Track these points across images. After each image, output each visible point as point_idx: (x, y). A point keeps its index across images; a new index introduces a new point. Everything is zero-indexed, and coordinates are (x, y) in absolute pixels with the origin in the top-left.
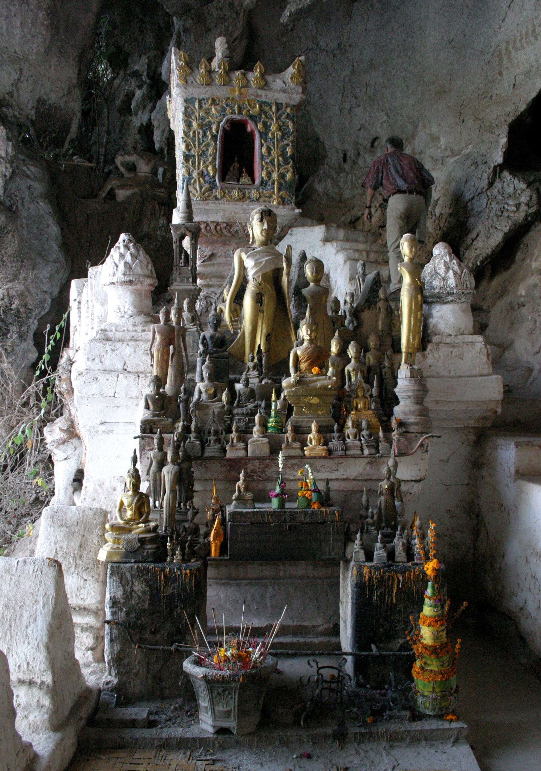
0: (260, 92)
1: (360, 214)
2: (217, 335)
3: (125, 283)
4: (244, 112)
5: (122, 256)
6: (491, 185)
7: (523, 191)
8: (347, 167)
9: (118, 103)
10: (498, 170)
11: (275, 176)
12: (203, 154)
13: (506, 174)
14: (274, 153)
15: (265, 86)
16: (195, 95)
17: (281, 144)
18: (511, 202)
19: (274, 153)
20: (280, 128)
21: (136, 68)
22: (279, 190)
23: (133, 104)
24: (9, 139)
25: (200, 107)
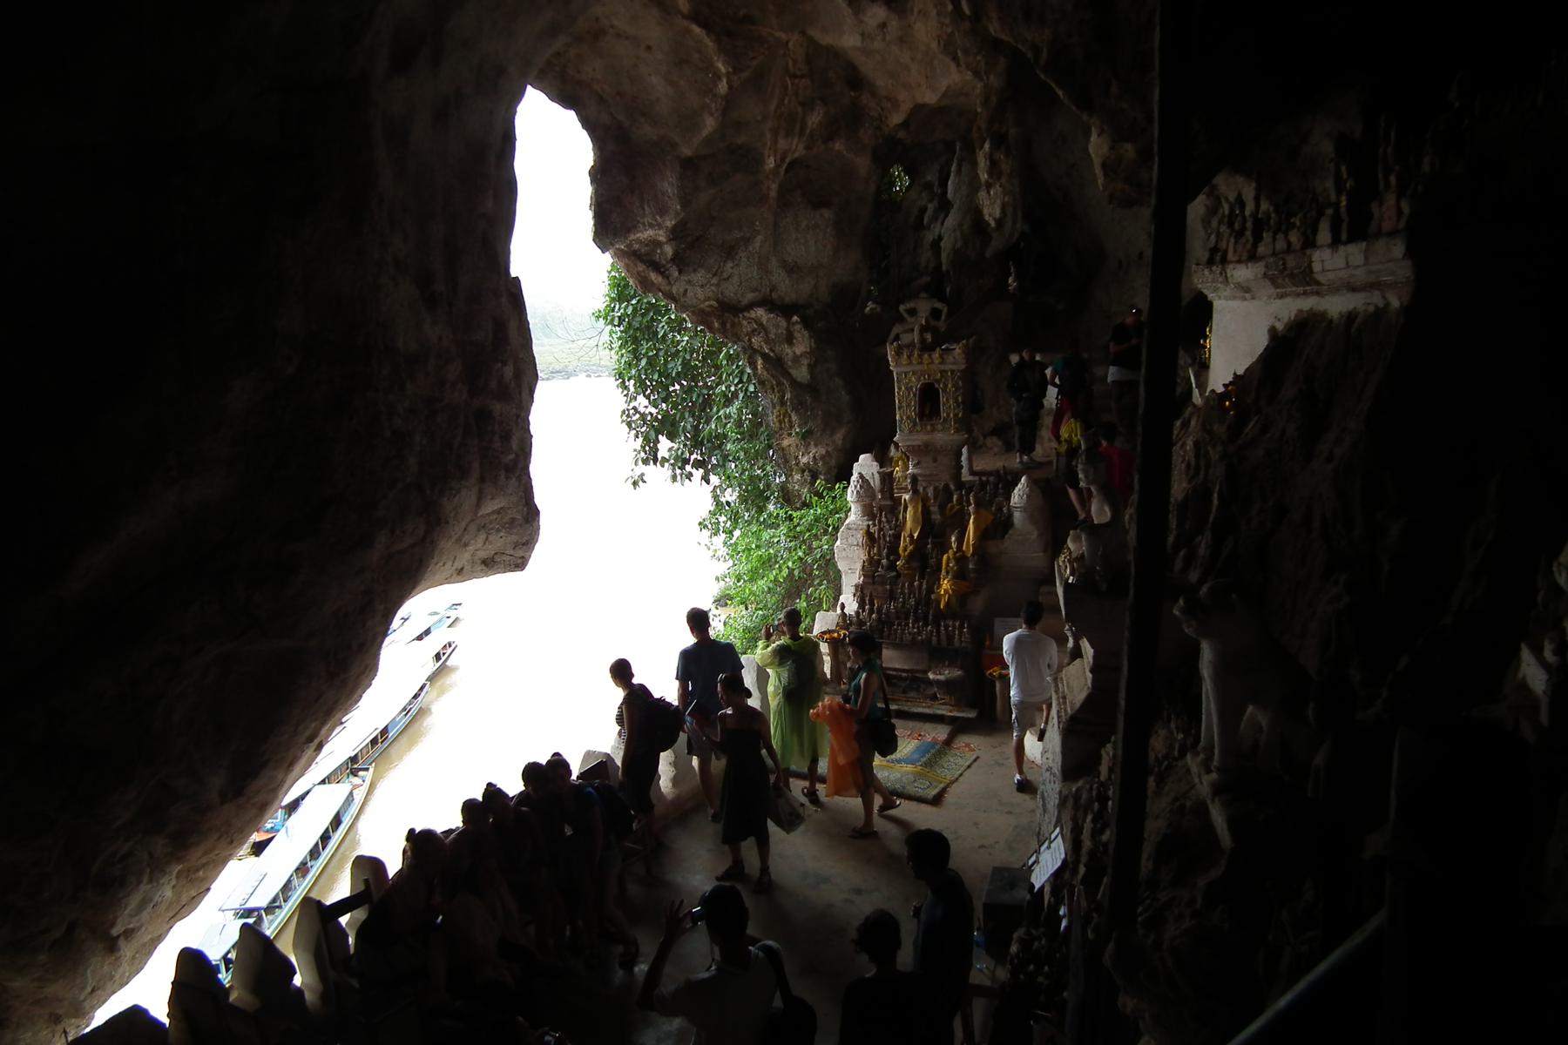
12: (909, 405)
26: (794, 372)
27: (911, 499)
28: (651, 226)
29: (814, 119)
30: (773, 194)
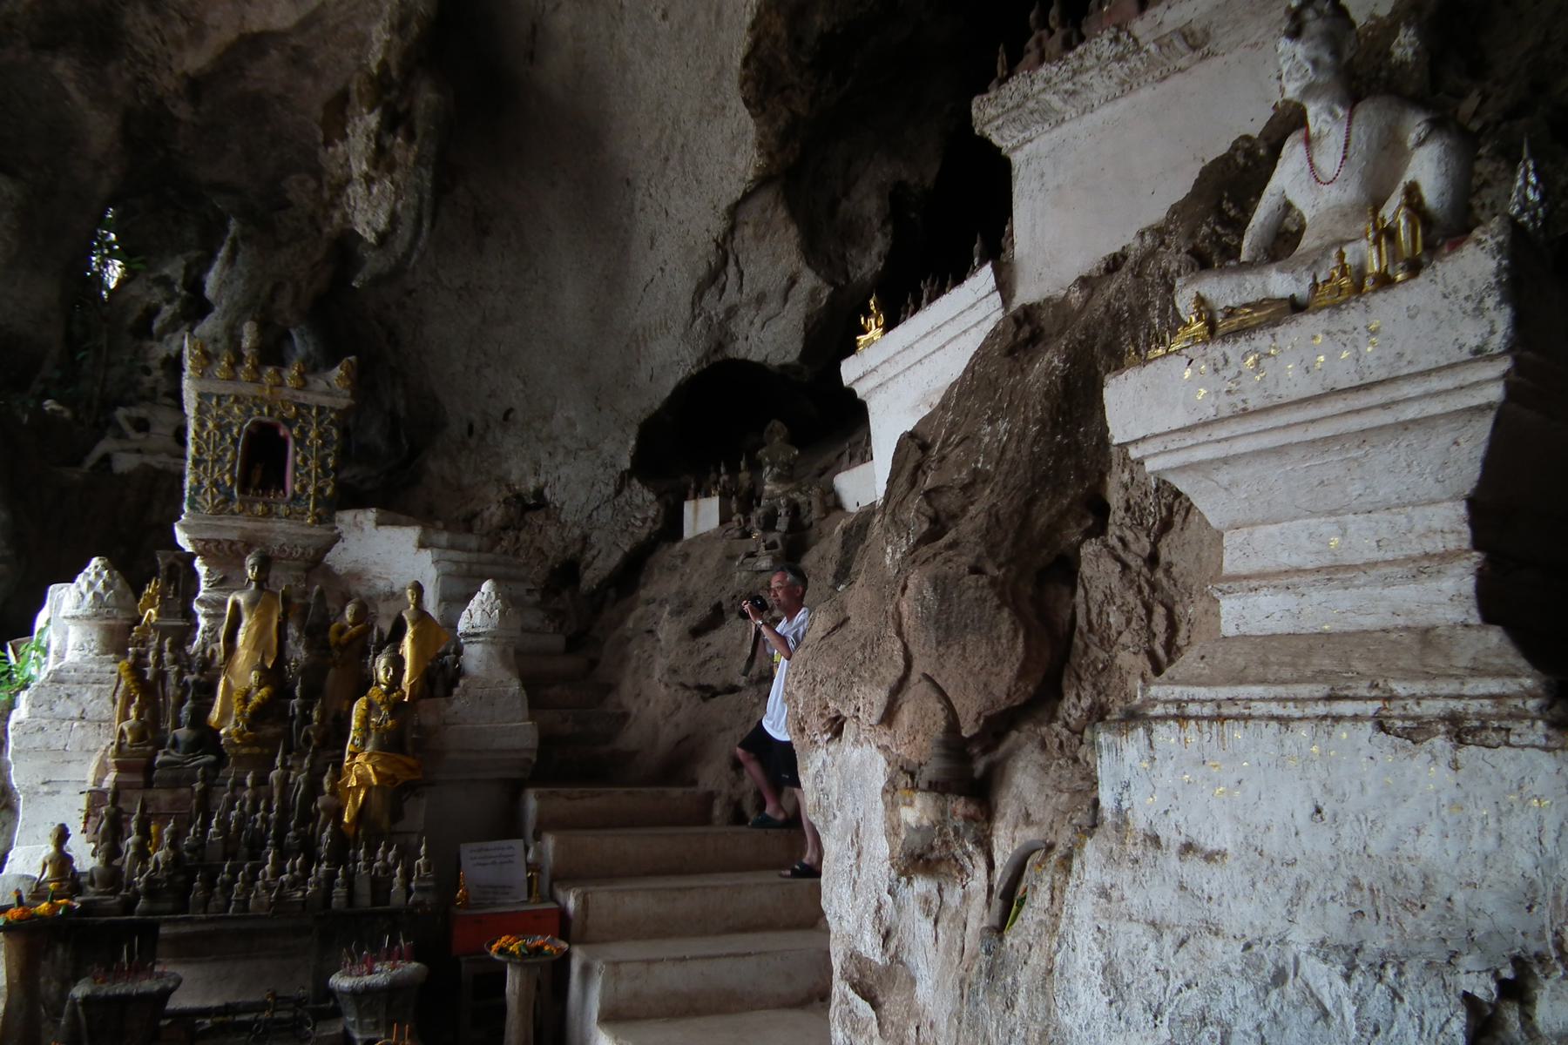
0: (297, 393)
3: (88, 618)
5: (91, 585)
6: (618, 492)
8: (473, 442)
9: (130, 320)
10: (624, 480)
11: (311, 490)
12: (218, 460)
13: (635, 481)
14: (312, 463)
15: (304, 385)
19: (312, 463)
20: (320, 436)
21: (166, 271)
22: (315, 506)
23: (157, 325)
25: (219, 404)
27: (252, 604)
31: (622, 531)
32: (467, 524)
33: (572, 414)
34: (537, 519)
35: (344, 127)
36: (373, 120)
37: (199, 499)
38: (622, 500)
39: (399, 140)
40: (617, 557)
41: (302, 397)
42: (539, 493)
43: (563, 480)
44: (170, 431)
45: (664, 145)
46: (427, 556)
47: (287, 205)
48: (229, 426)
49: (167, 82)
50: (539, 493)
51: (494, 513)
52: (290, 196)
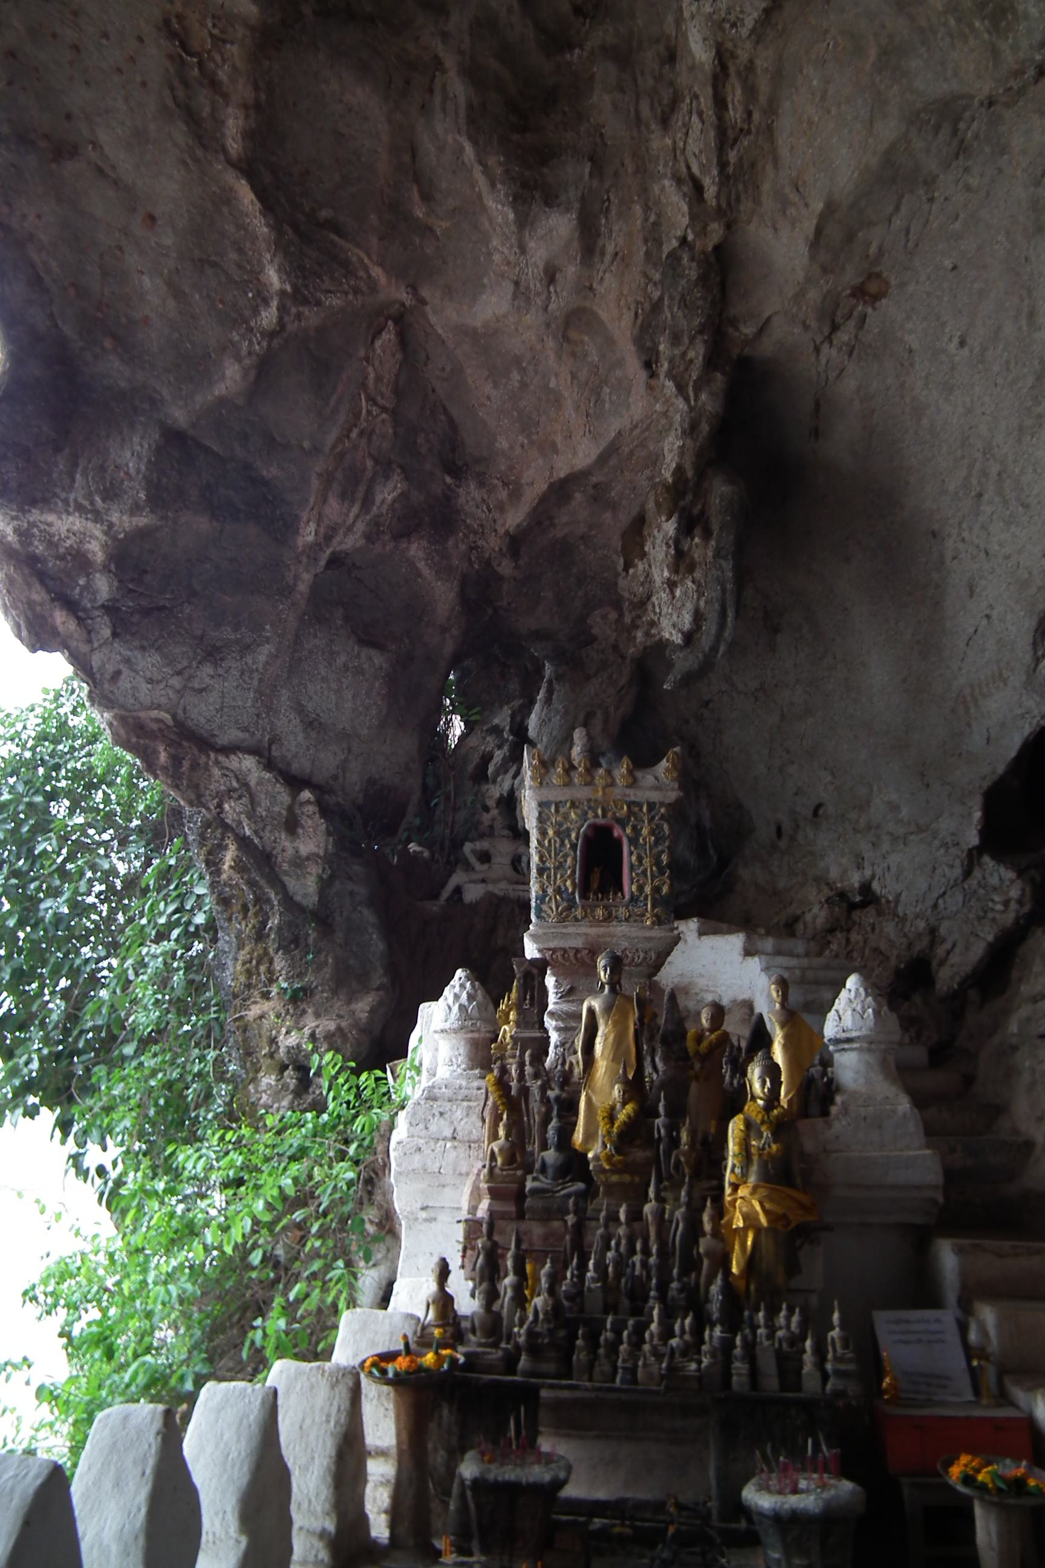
0: (628, 791)
1: (799, 912)
2: (564, 1095)
3: (455, 1031)
4: (610, 815)
5: (457, 997)
6: (967, 874)
7: (1012, 882)
8: (783, 844)
9: (471, 767)
10: (973, 858)
11: (648, 889)
12: (560, 866)
13: (986, 859)
14: (647, 862)
15: (633, 783)
16: (551, 798)
17: (655, 851)
18: (996, 898)
19: (647, 862)
20: (652, 832)
21: (496, 721)
22: (653, 907)
23: (491, 769)
24: (329, 834)
25: (557, 811)
26: (291, 884)
27: (608, 1009)
28: (79, 508)
29: (387, 493)
30: (303, 587)
31: (980, 919)
32: (789, 928)
33: (894, 797)
34: (868, 916)
35: (642, 546)
36: (670, 527)
37: (544, 907)
38: (973, 882)
39: (697, 540)
40: (978, 951)
41: (633, 795)
42: (866, 888)
43: (894, 869)
44: (507, 861)
45: (974, 481)
46: (755, 964)
47: (593, 639)
48: (568, 830)
49: (493, 543)
50: (866, 888)
51: (817, 915)
52: (595, 631)
